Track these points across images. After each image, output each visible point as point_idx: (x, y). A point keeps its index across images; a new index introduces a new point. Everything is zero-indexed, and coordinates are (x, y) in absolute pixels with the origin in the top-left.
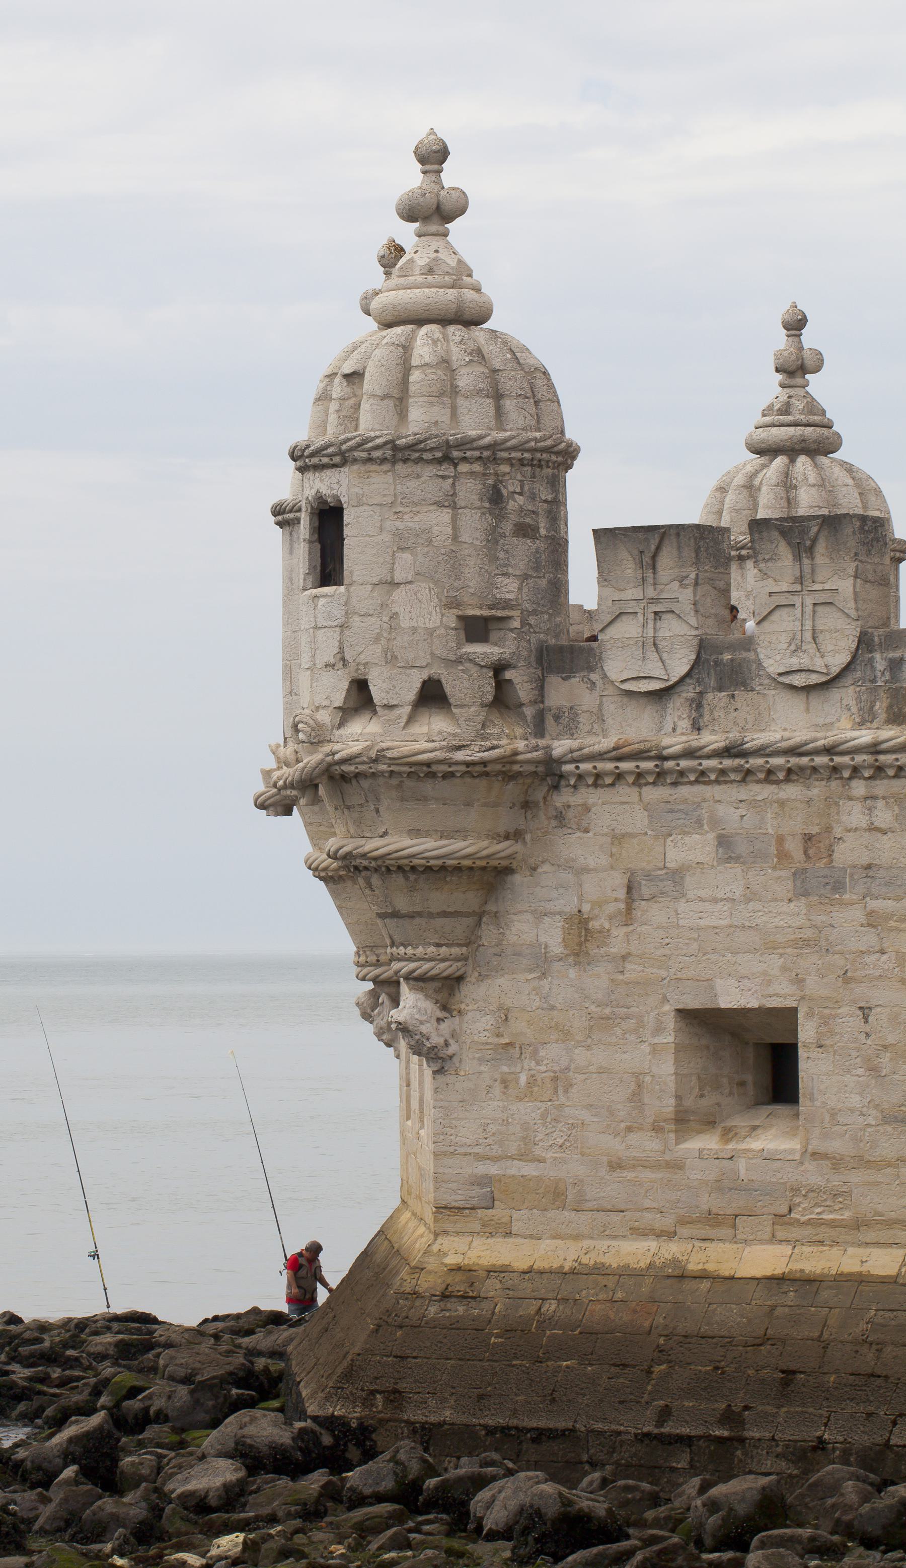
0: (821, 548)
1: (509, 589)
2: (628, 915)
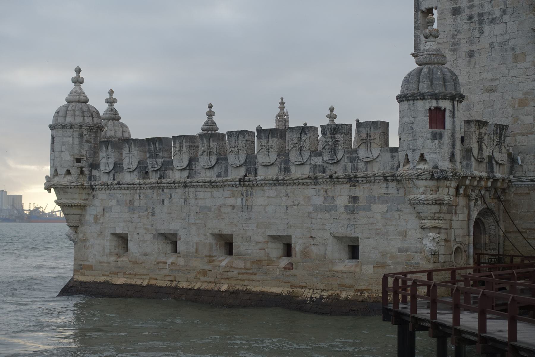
0: (133, 145)
1: (84, 153)
2: (103, 215)
